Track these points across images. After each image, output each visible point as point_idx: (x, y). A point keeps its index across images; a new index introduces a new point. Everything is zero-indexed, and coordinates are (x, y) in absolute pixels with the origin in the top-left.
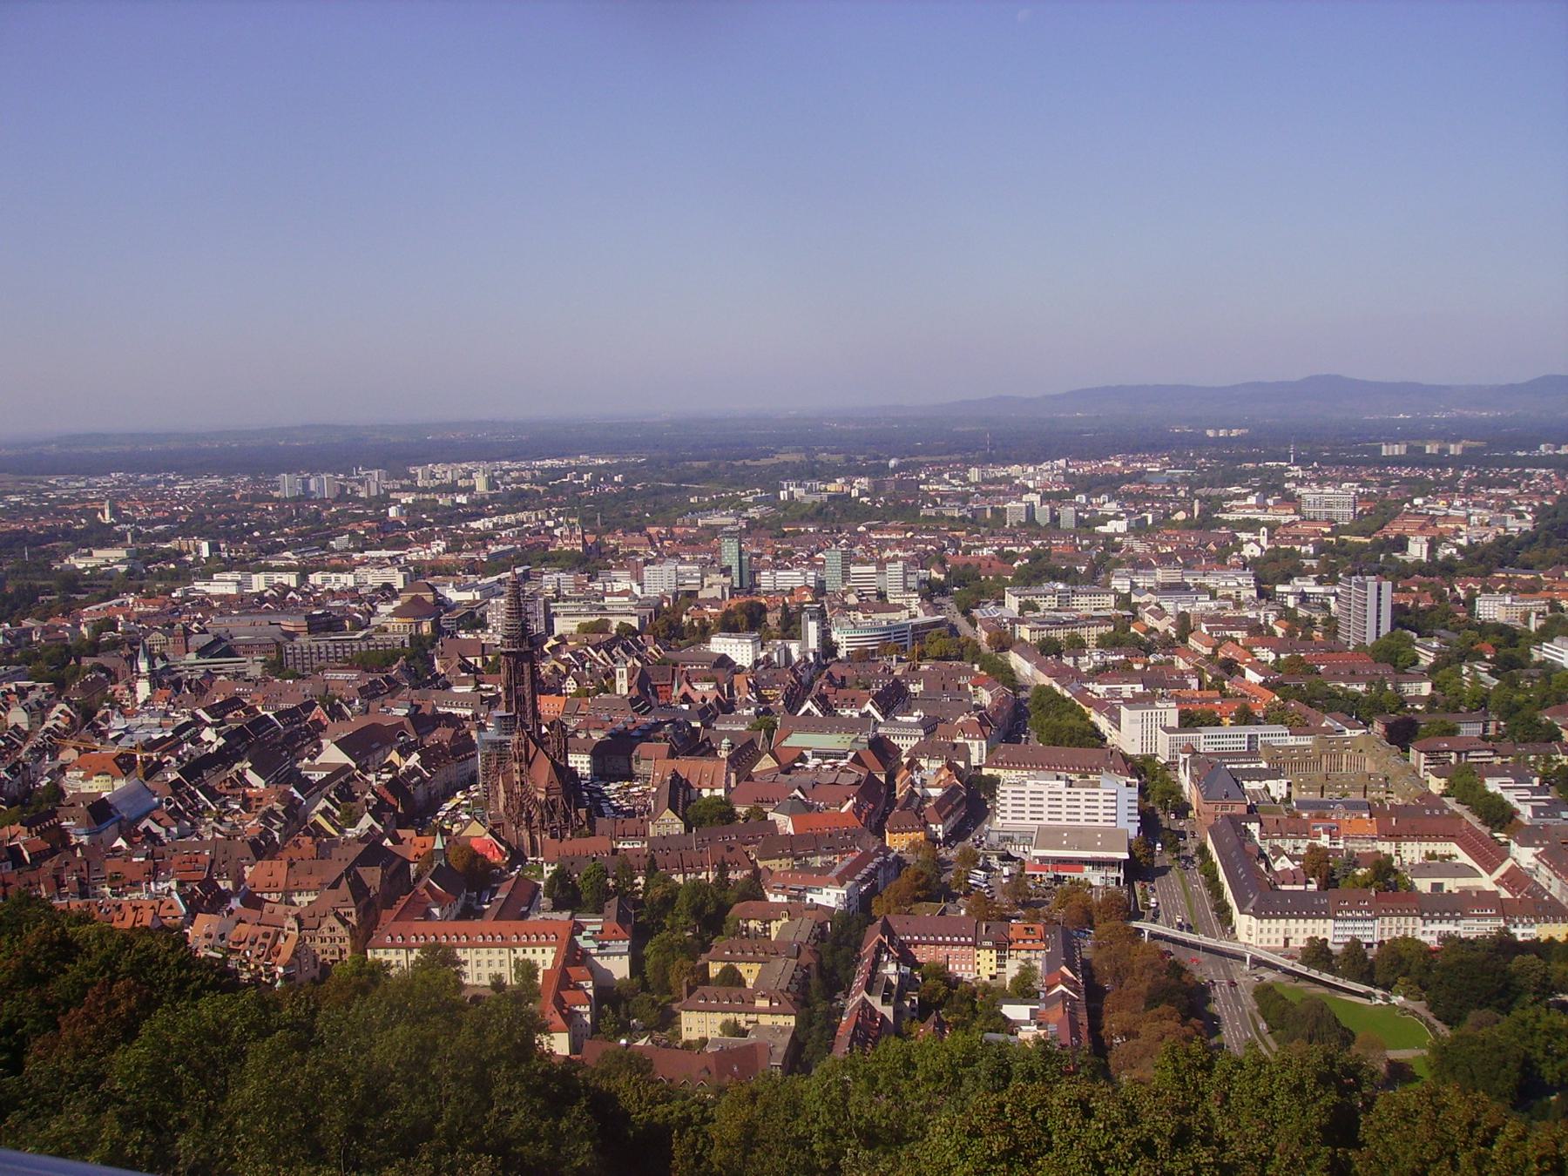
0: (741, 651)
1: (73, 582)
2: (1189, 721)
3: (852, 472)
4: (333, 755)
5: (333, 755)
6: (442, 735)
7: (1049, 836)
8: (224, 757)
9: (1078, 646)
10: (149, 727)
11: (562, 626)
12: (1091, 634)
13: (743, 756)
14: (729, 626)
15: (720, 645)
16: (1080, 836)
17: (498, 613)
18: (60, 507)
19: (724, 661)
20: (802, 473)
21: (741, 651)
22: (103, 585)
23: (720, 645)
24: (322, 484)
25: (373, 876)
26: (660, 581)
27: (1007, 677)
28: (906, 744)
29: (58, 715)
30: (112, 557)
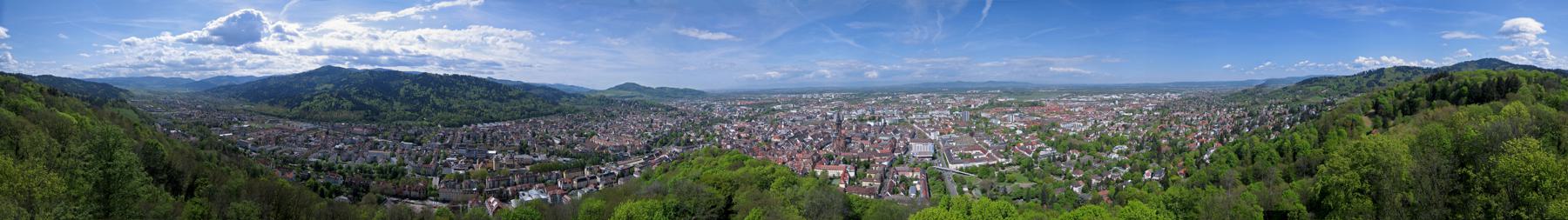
0: (872, 124)
1: (774, 110)
2: (941, 134)
3: (888, 95)
4: (810, 138)
5: (810, 138)
6: (827, 136)
7: (920, 153)
8: (793, 137)
9: (924, 123)
10: (783, 132)
11: (845, 119)
12: (926, 121)
13: (872, 142)
14: (870, 120)
15: (868, 123)
16: (925, 153)
17: (835, 116)
18: (773, 99)
19: (869, 125)
20: (881, 96)
21: (872, 124)
22: (779, 110)
23: (868, 123)
24: (809, 96)
25: (815, 158)
26: (860, 112)
27: (912, 128)
28: (897, 139)
29: (771, 129)
30: (779, 107)
